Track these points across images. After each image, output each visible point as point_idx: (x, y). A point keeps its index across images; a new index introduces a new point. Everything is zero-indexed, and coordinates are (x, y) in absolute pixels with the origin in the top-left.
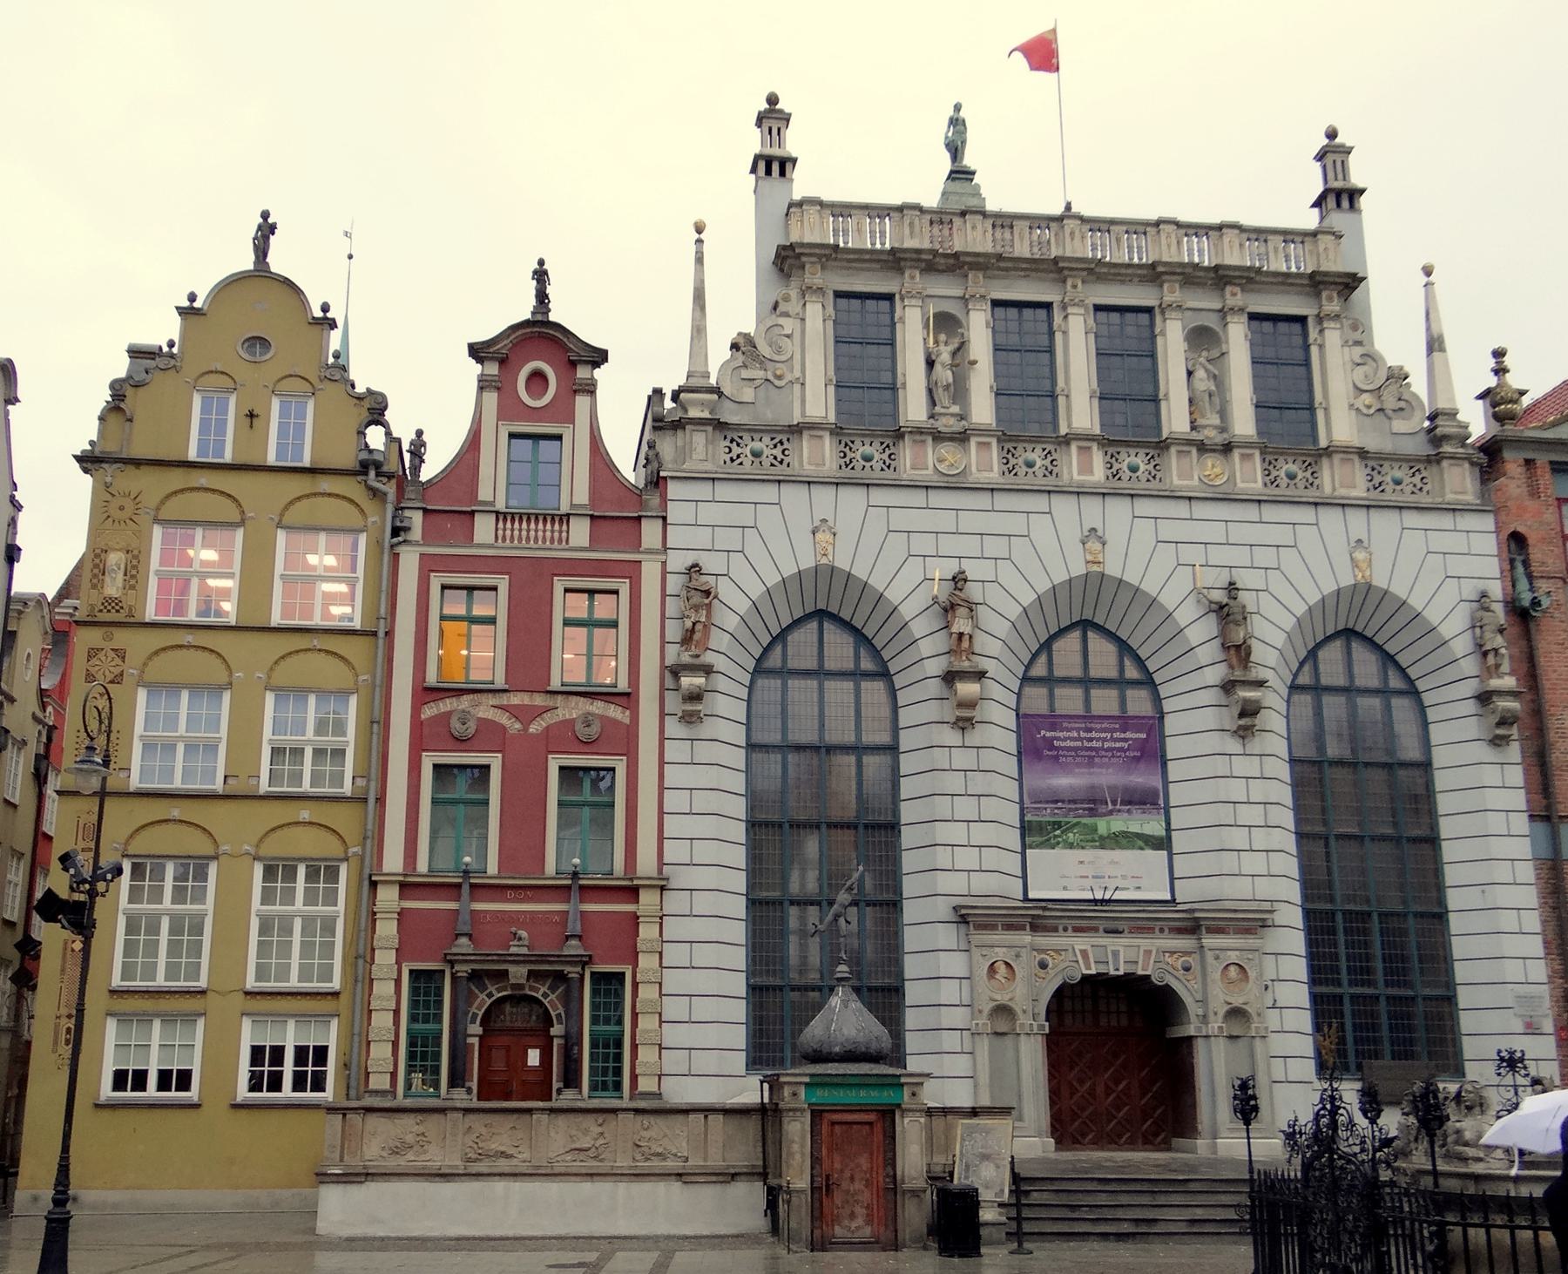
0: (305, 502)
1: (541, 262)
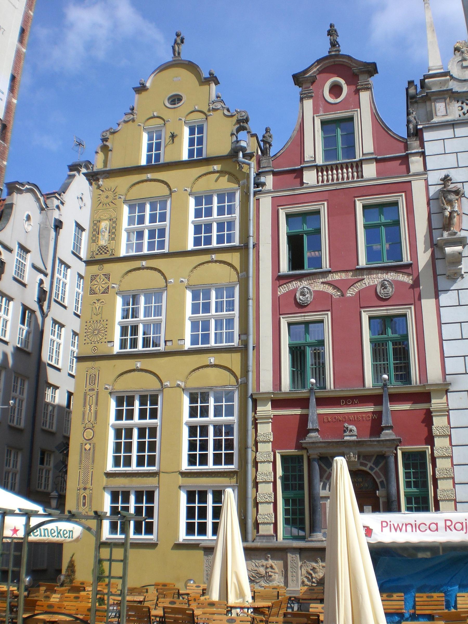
0: (204, 178)
1: (331, 26)
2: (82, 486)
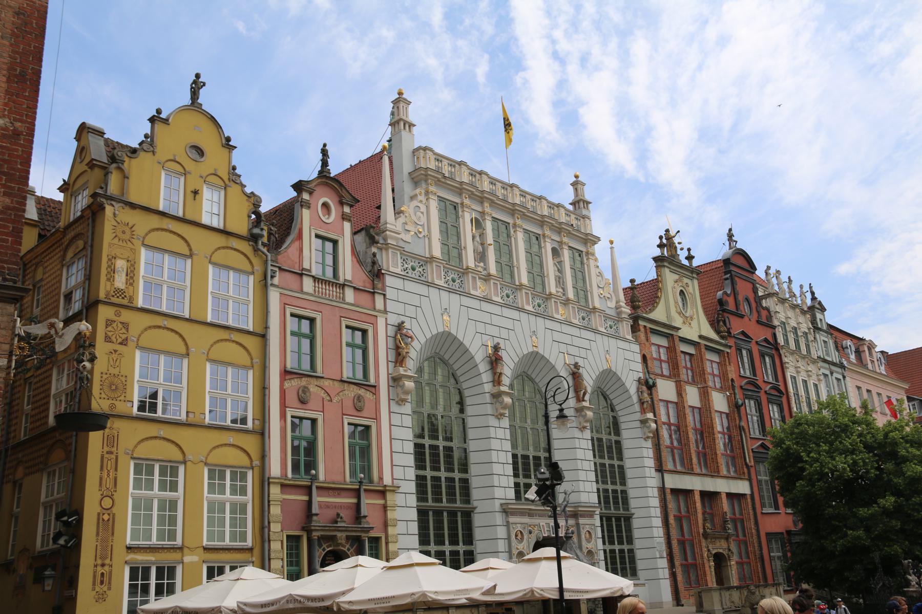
1: (325, 145)
2: (99, 562)
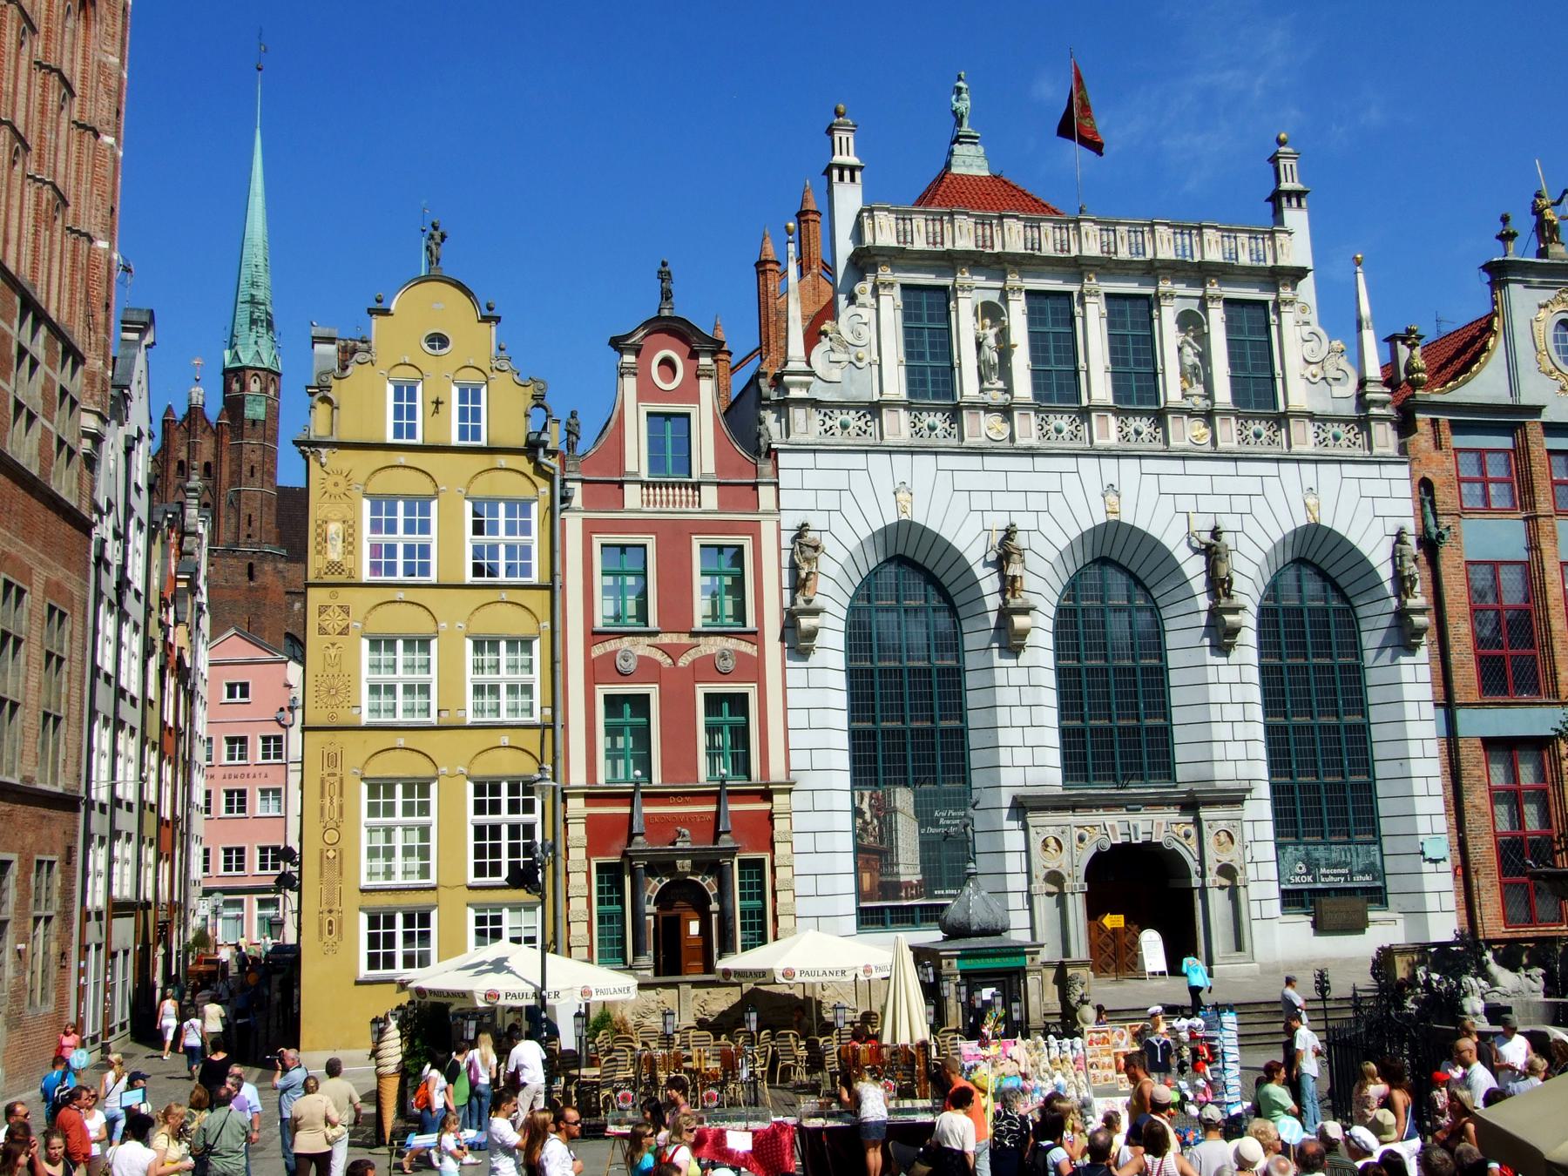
0: (486, 475)
1: (664, 264)
2: (325, 908)
